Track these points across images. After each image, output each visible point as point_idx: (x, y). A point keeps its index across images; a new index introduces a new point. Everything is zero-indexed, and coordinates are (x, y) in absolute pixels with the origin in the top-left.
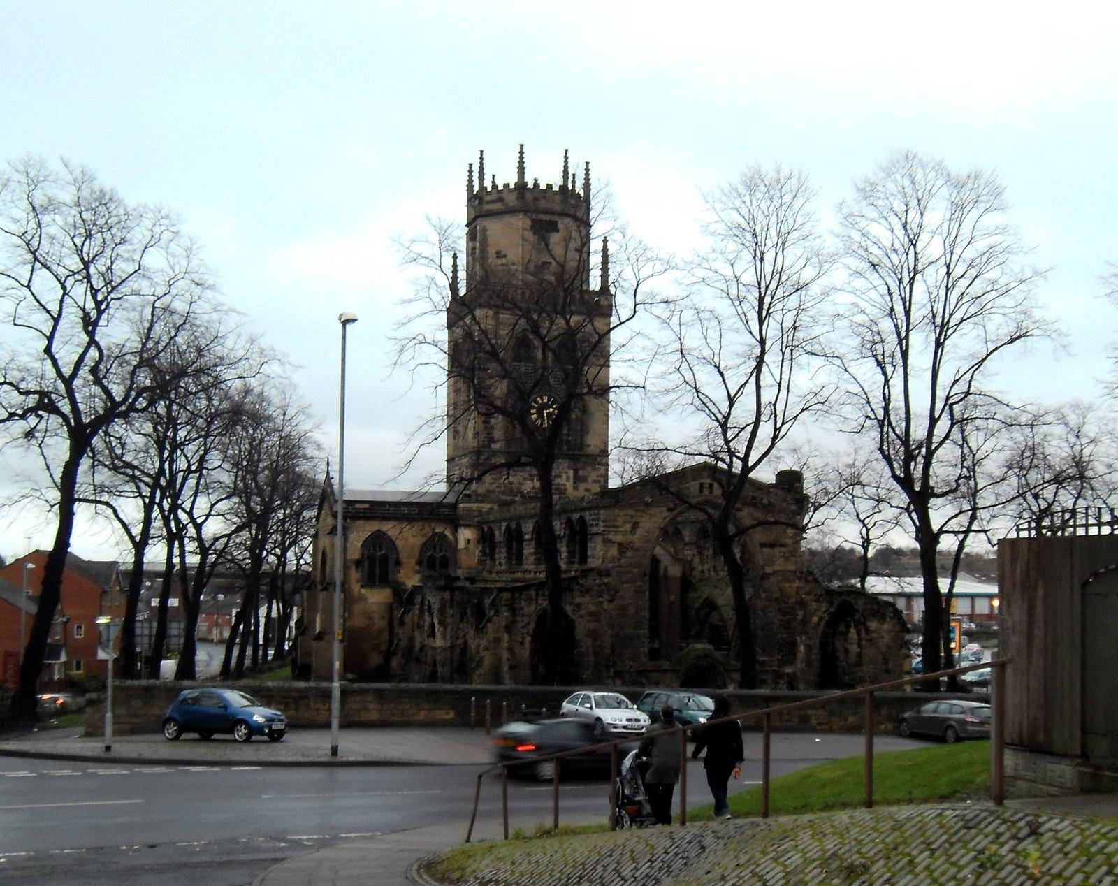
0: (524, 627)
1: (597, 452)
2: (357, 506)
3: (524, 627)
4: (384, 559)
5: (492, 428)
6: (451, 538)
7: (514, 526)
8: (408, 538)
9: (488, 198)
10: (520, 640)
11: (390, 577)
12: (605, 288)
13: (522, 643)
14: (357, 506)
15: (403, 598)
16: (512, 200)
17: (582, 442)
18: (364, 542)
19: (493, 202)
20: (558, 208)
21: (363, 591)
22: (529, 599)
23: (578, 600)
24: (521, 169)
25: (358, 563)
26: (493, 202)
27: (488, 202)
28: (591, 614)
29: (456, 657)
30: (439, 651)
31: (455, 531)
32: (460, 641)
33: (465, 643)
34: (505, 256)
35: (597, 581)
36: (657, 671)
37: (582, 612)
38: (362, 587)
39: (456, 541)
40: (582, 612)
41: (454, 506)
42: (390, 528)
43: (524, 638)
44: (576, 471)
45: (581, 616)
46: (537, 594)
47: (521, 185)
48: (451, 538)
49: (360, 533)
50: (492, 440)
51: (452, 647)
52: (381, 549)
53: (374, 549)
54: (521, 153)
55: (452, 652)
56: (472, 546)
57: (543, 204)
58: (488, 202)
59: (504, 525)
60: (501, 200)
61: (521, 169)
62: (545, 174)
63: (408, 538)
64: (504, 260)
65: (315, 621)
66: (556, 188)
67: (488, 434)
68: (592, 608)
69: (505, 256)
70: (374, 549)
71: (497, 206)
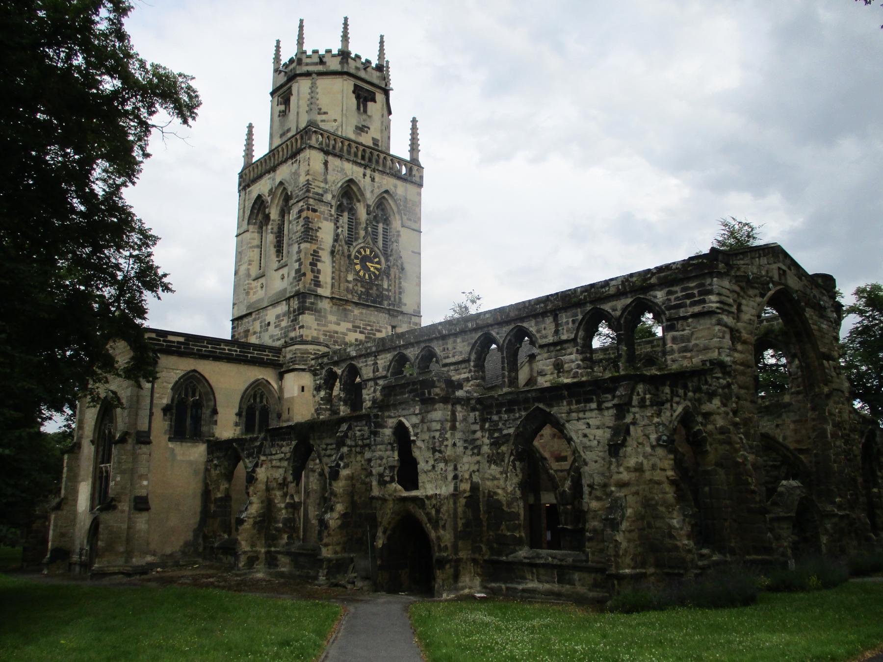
1: (411, 312)
2: (170, 338)
4: (198, 405)
5: (319, 272)
6: (275, 386)
7: (412, 353)
8: (229, 383)
9: (308, 60)
11: (204, 429)
12: (414, 163)
14: (170, 338)
15: (226, 453)
16: (334, 65)
17: (400, 299)
18: (177, 382)
19: (316, 64)
20: (376, 81)
21: (171, 445)
24: (345, 38)
25: (166, 410)
26: (316, 64)
27: (307, 64)
29: (460, 510)
31: (281, 376)
32: (465, 486)
33: (475, 488)
34: (325, 113)
38: (170, 440)
39: (281, 389)
41: (277, 351)
42: (209, 369)
44: (394, 327)
45: (710, 434)
46: (672, 391)
47: (344, 55)
48: (275, 386)
49: (172, 370)
50: (317, 284)
51: (455, 495)
52: (194, 395)
53: (186, 395)
55: (455, 503)
56: (308, 393)
57: (362, 74)
58: (307, 64)
59: (384, 360)
60: (321, 62)
61: (345, 38)
62: (364, 49)
63: (229, 383)
64: (324, 117)
65: (74, 492)
66: (374, 65)
67: (315, 277)
69: (325, 113)
70: (186, 395)
71: (320, 68)
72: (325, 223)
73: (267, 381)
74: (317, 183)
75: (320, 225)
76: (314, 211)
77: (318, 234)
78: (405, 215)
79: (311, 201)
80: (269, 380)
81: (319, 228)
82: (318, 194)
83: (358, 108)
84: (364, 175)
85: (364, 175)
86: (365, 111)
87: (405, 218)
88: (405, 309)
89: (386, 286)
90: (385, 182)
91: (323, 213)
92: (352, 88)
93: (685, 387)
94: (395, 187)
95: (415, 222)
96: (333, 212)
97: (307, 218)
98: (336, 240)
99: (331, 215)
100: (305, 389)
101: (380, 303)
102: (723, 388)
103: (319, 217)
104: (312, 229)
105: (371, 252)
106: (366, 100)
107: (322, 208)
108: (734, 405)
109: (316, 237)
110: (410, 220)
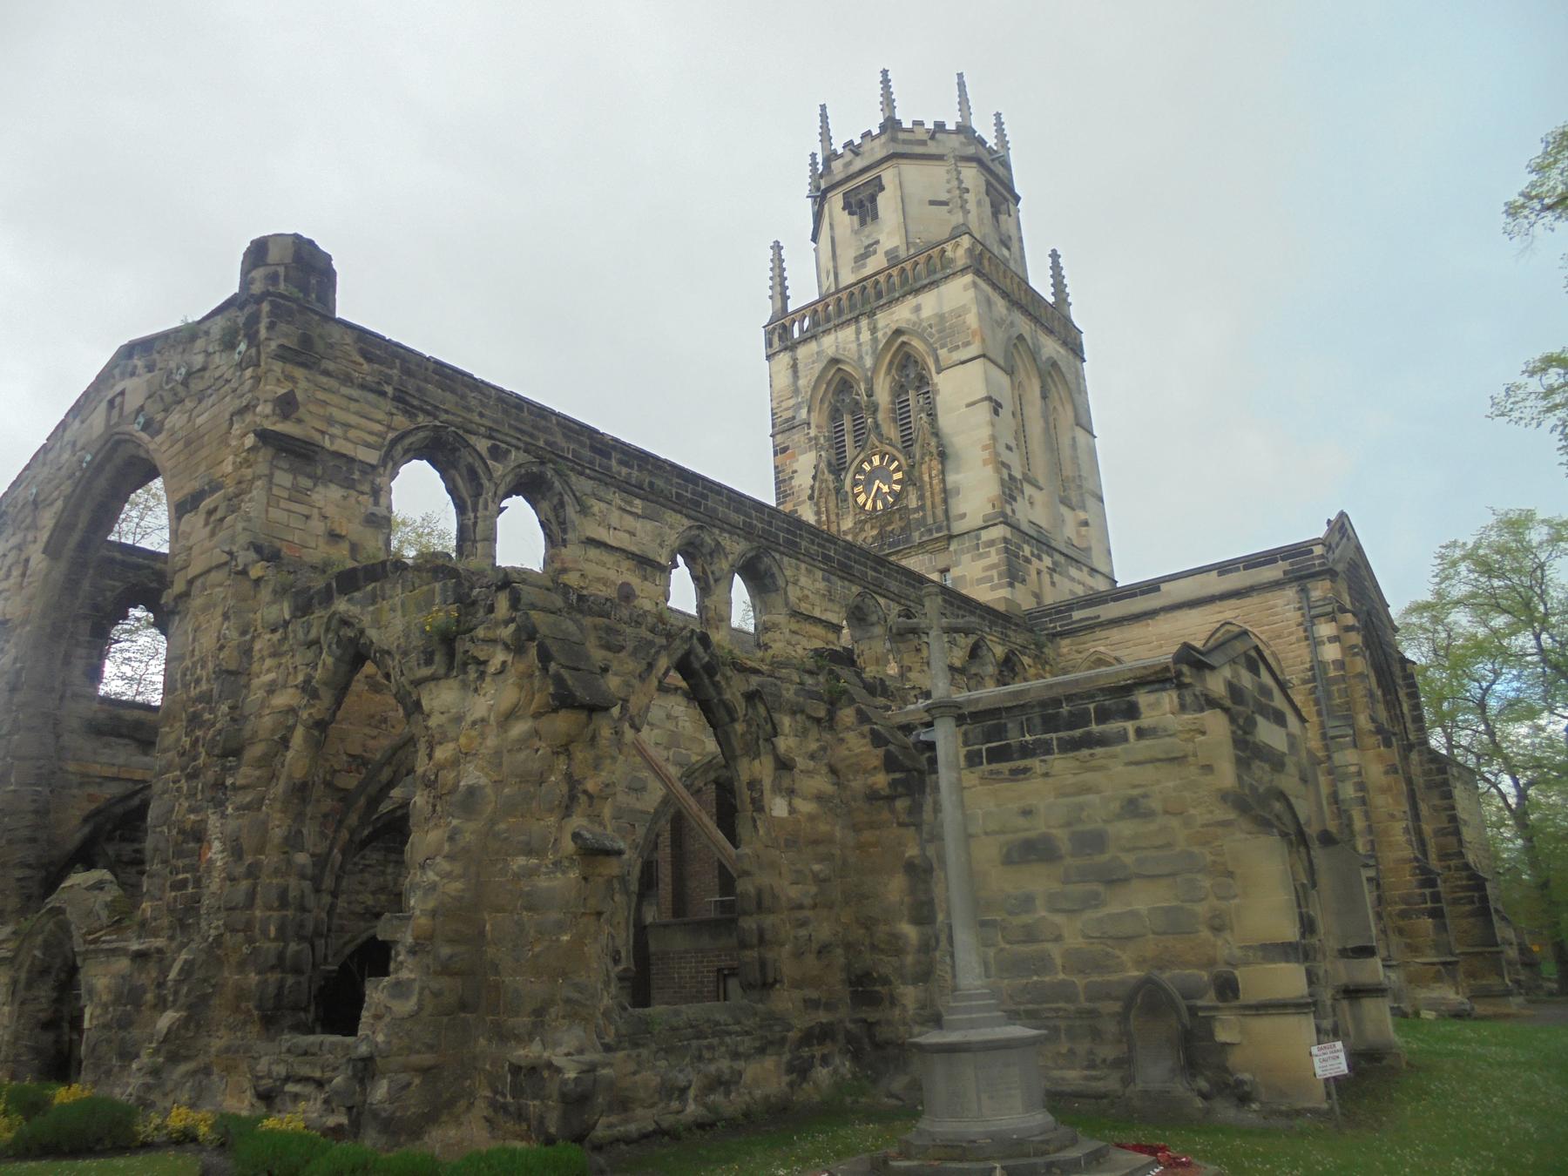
54: (824, 117)
61: (825, 135)
74: (784, 405)
75: (795, 466)
77: (794, 483)
78: (942, 347)
82: (787, 421)
83: (863, 223)
84: (858, 332)
85: (858, 332)
86: (875, 217)
87: (942, 353)
88: (958, 527)
89: (913, 502)
90: (895, 317)
92: (841, 204)
94: (918, 309)
95: (967, 344)
98: (814, 478)
101: (907, 540)
103: (793, 456)
105: (882, 459)
106: (873, 199)
107: (798, 437)
110: (957, 347)
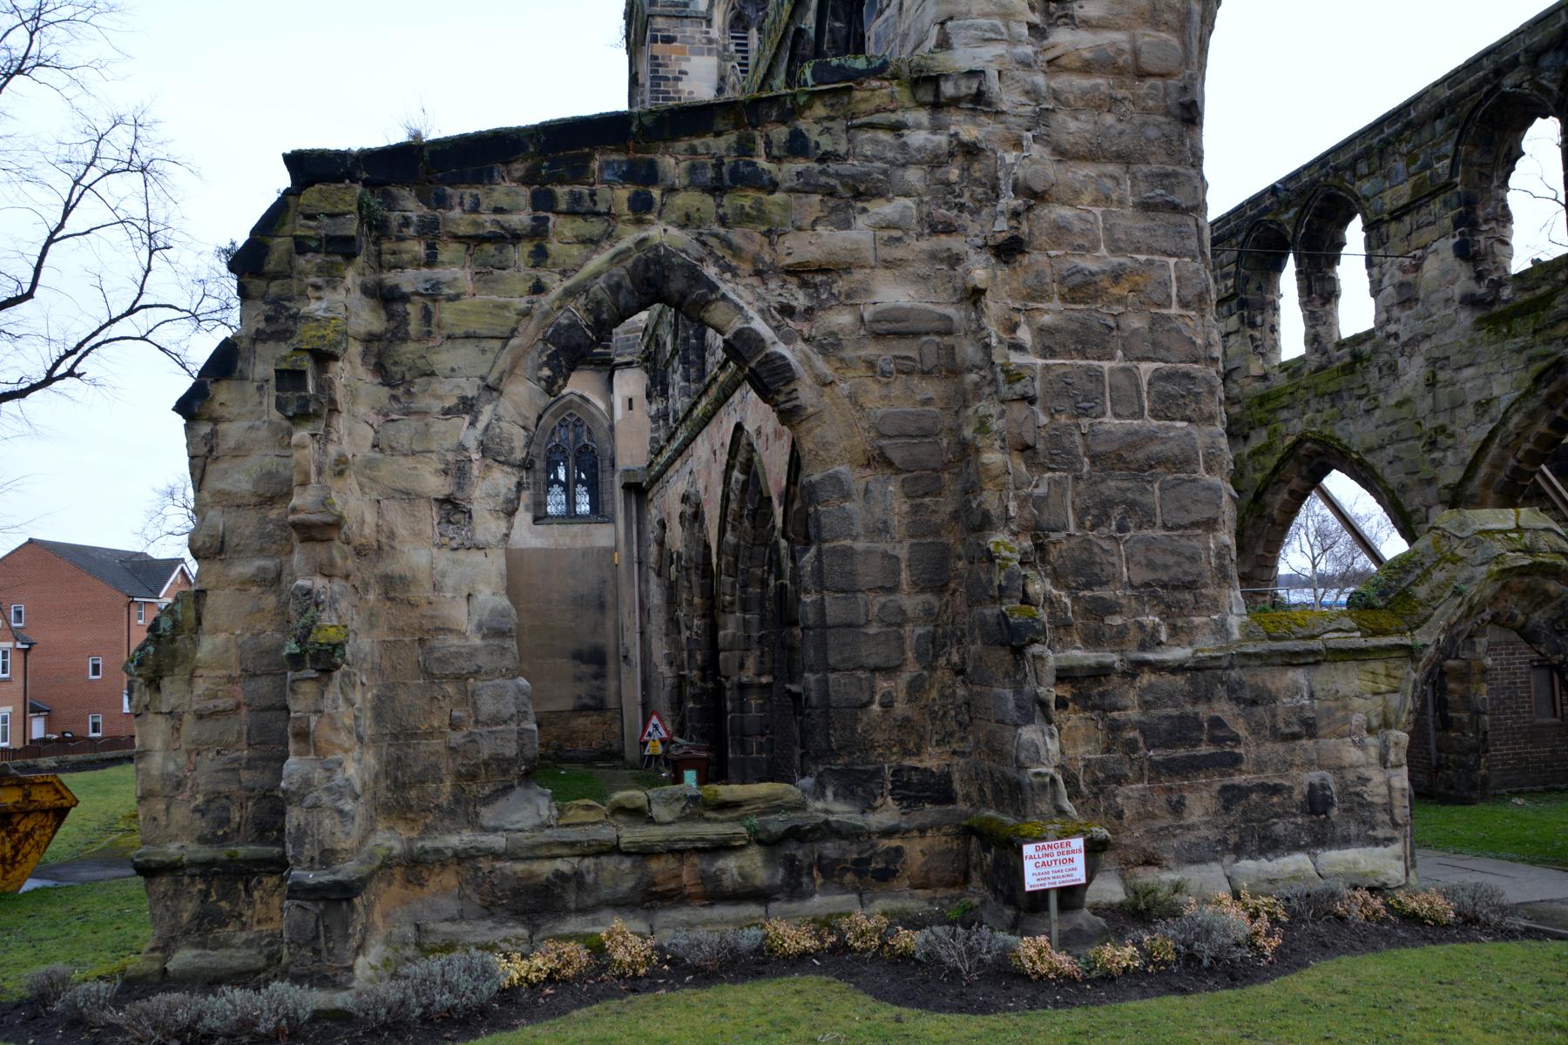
0: (467, 406)
3: (467, 406)
6: (601, 405)
10: (437, 485)
13: (452, 508)
22: (487, 244)
23: (801, 247)
28: (891, 328)
30: (178, 607)
35: (917, 138)
36: (1292, 660)
37: (842, 319)
40: (842, 319)
43: (459, 471)
45: (829, 345)
46: (542, 201)
48: (601, 405)
68: (893, 294)
72: (695, 60)
73: (581, 397)
75: (684, 66)
76: (669, 40)
77: (681, 85)
79: (660, 23)
80: (586, 394)
81: (685, 73)
91: (685, 40)
93: (642, 175)
96: (715, 33)
97: (654, 58)
99: (710, 41)
100: (635, 403)
102: (935, 162)
103: (682, 51)
104: (667, 79)
107: (690, 30)
108: (1002, 225)
109: (677, 92)
